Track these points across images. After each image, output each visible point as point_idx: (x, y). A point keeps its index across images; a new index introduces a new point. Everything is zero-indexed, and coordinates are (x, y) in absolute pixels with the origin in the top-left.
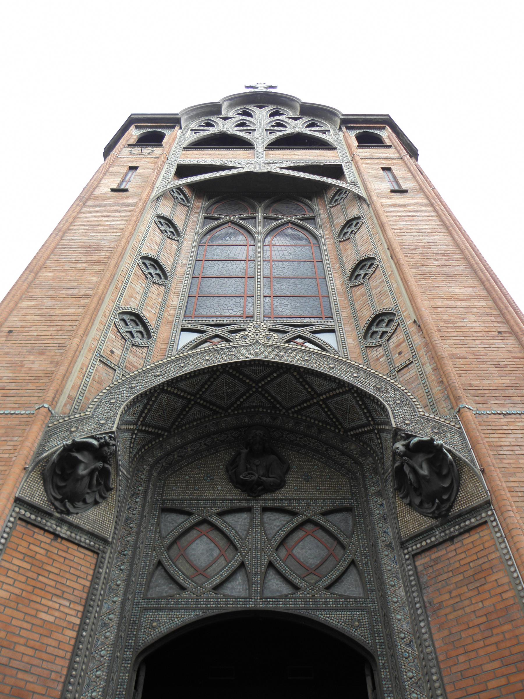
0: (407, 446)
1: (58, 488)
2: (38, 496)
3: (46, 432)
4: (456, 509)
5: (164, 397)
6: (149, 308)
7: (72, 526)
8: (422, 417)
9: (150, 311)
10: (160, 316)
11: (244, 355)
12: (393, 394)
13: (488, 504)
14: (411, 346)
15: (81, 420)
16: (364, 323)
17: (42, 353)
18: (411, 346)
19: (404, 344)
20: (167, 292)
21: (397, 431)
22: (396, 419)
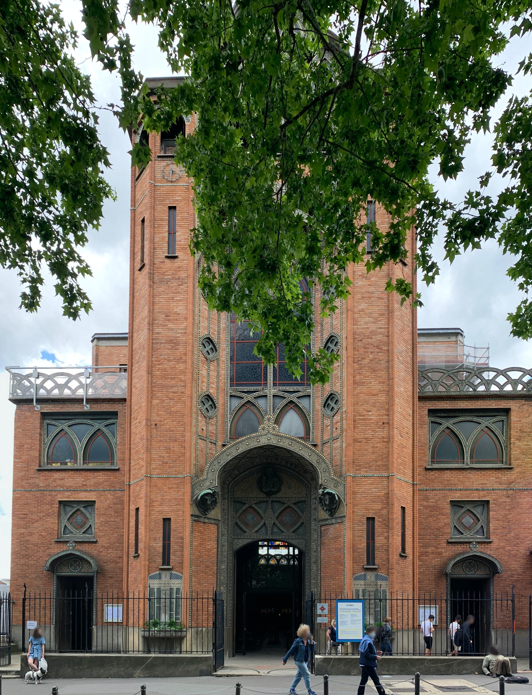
0: (323, 492)
1: (202, 508)
2: (197, 513)
3: (192, 487)
4: (337, 515)
5: (231, 463)
6: (212, 385)
7: (208, 518)
8: (332, 479)
9: (212, 387)
10: (218, 388)
11: (264, 441)
12: (324, 465)
13: (345, 516)
14: (342, 426)
15: (203, 481)
16: (325, 398)
17: (176, 441)
18: (342, 426)
19: (339, 424)
20: (218, 364)
21: (321, 485)
22: (322, 478)
